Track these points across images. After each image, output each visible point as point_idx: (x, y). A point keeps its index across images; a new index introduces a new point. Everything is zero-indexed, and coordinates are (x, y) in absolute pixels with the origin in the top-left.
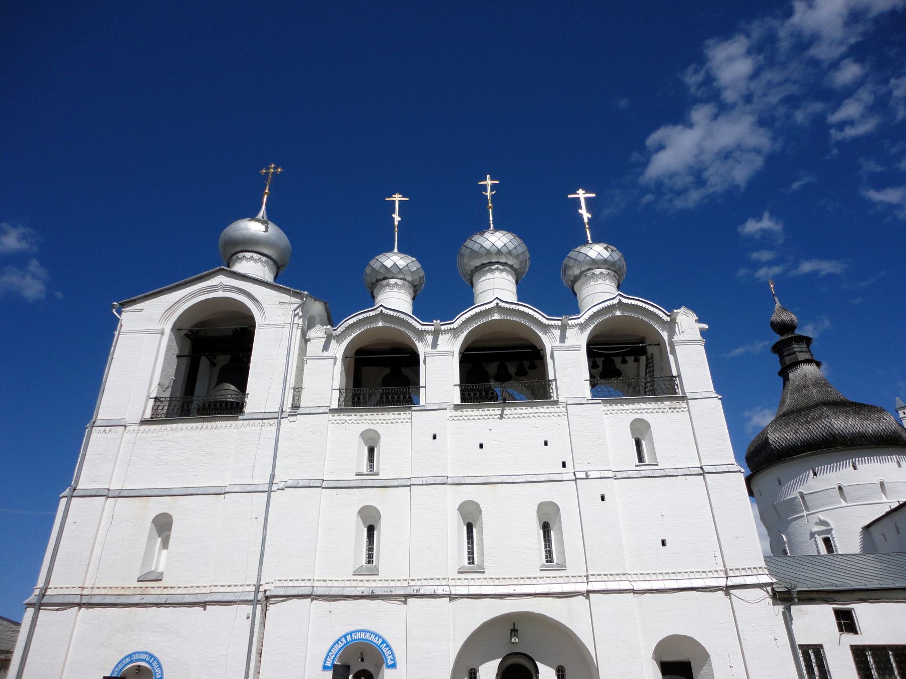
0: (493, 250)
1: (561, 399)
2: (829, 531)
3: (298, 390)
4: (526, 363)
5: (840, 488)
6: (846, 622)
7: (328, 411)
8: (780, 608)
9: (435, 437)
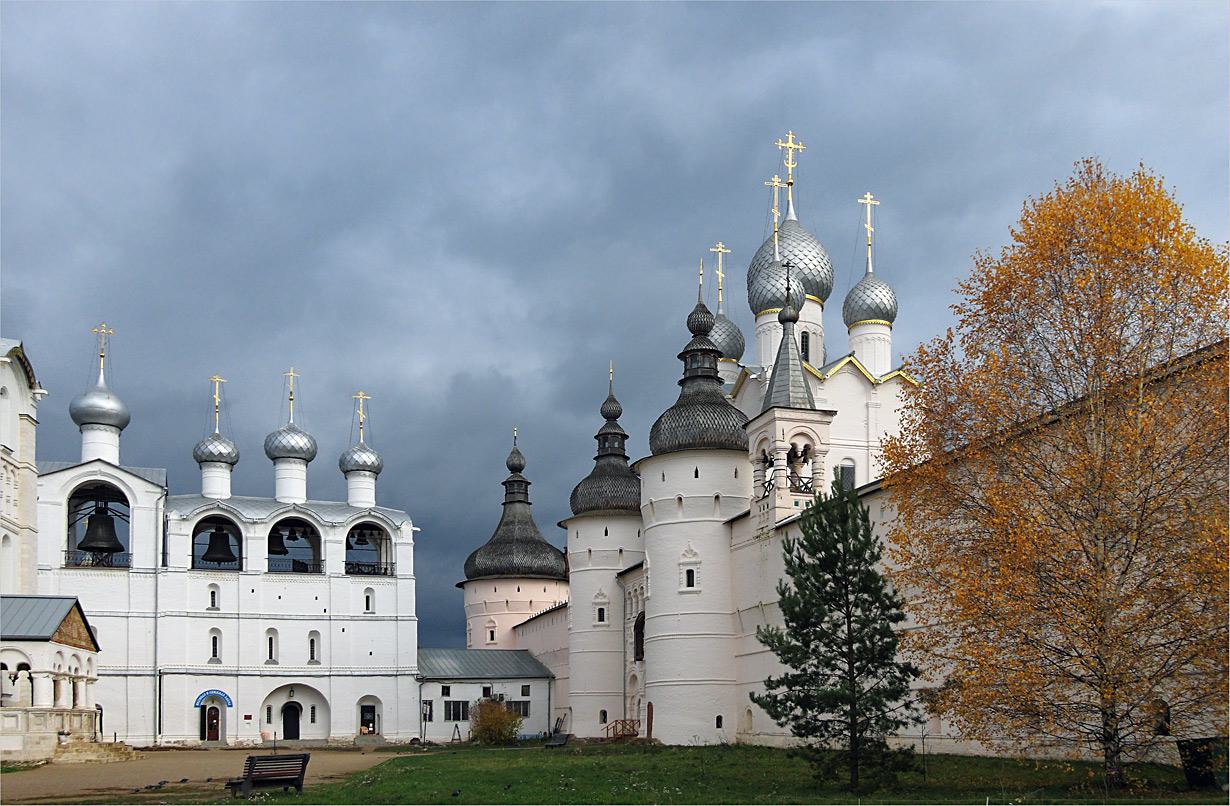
0: (297, 448)
1: (328, 573)
2: (494, 627)
4: (309, 530)
6: (446, 691)
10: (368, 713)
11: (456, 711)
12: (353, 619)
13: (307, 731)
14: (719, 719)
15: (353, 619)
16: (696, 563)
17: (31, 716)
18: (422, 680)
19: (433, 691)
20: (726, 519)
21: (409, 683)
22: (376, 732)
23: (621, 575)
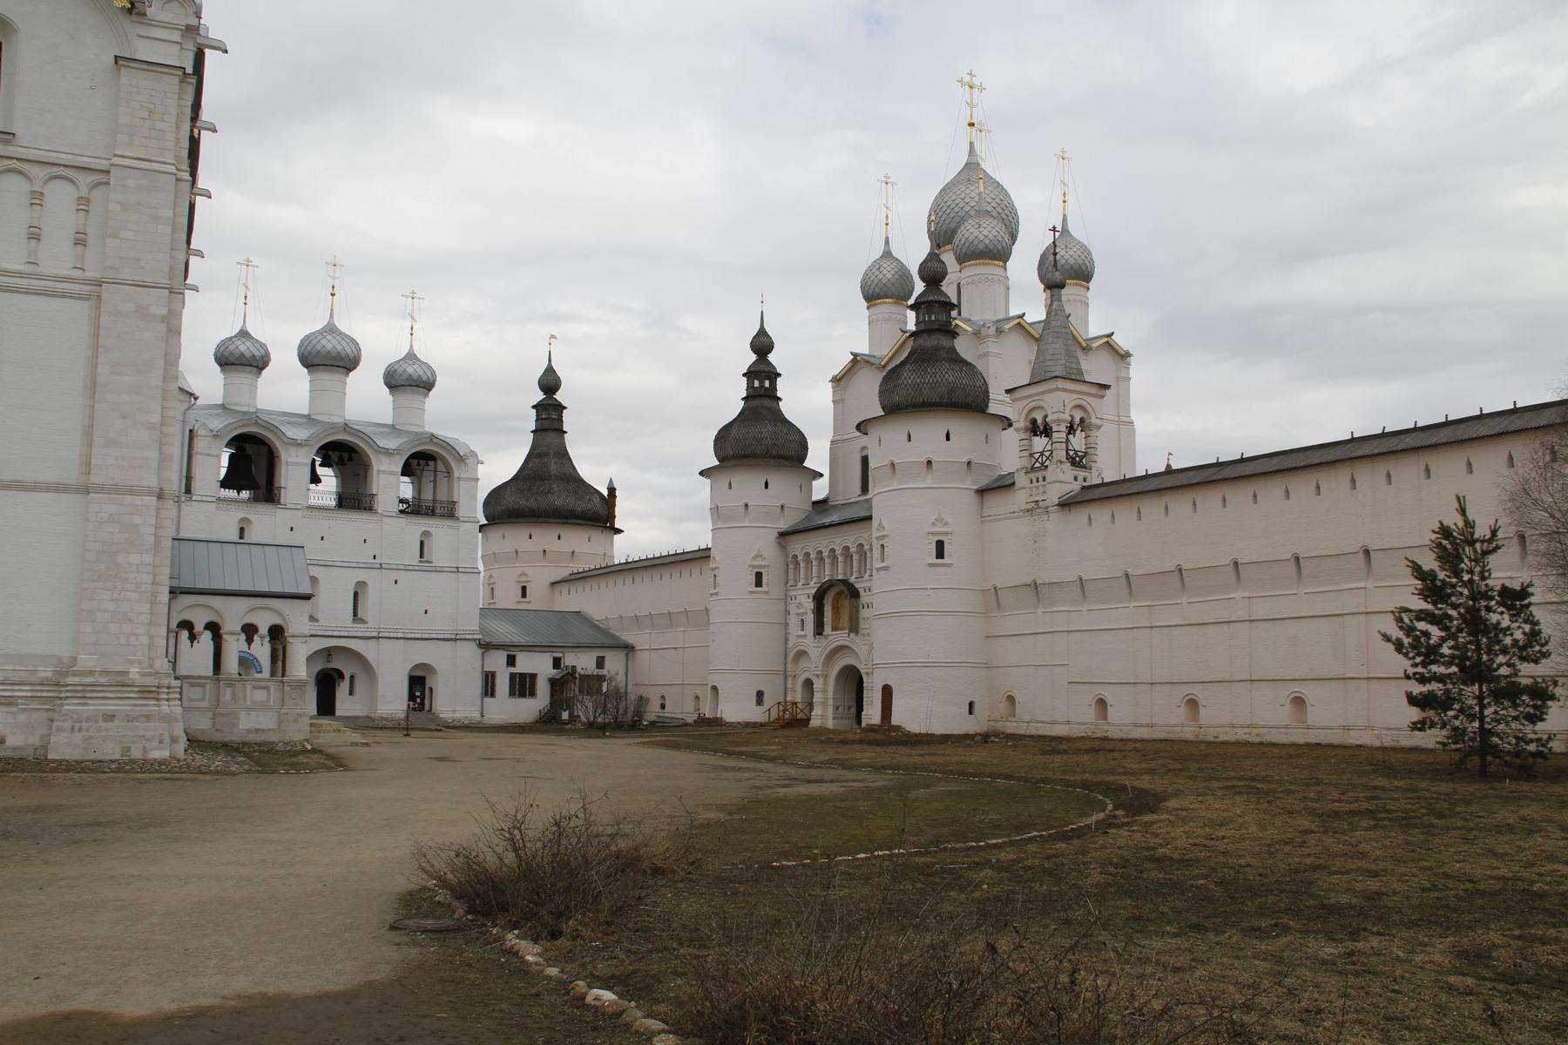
1: (380, 511)
3: (189, 479)
4: (346, 455)
5: (545, 551)
6: (511, 661)
7: (214, 499)
8: (481, 651)
9: (292, 529)
10: (418, 684)
11: (523, 686)
12: (407, 569)
13: (346, 704)
14: (971, 704)
15: (407, 569)
16: (947, 534)
17: (287, 689)
18: (486, 646)
19: (497, 661)
20: (976, 488)
21: (470, 652)
22: (427, 707)
23: (783, 535)
